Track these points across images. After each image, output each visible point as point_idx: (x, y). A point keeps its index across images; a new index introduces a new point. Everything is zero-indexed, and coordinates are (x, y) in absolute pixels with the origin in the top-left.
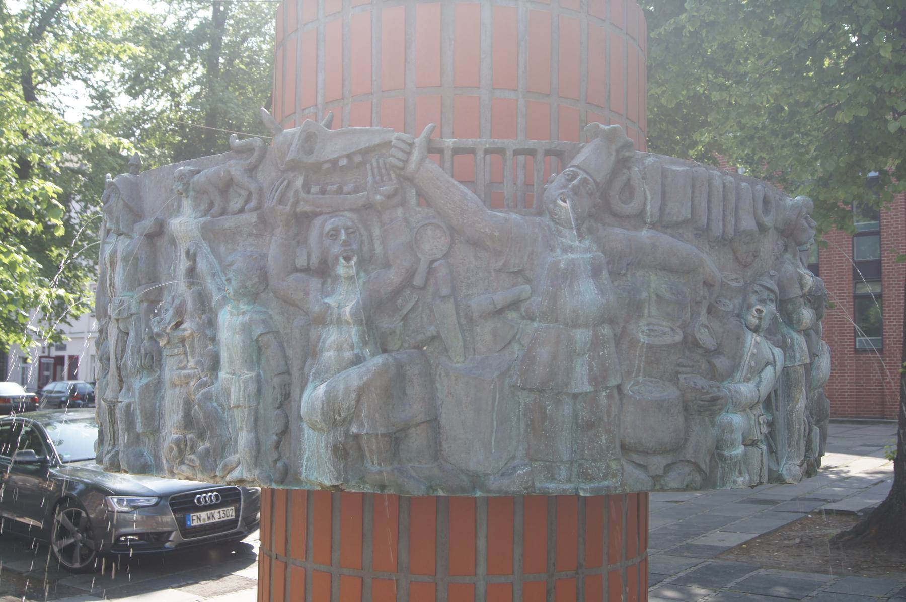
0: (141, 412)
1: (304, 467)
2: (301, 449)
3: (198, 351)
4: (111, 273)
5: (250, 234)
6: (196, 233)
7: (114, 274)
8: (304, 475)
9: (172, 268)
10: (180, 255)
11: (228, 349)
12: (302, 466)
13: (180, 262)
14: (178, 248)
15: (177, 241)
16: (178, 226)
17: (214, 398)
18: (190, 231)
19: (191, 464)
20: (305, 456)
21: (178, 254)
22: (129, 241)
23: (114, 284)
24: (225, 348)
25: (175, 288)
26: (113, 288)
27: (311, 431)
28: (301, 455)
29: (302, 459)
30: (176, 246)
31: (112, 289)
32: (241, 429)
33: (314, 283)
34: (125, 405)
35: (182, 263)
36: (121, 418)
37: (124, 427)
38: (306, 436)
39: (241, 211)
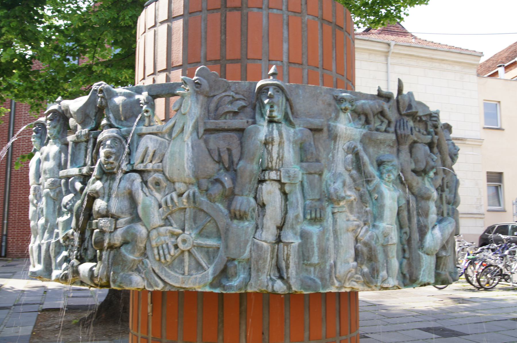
0: (319, 249)
1: (421, 275)
2: (421, 266)
3: (356, 210)
4: (279, 151)
5: (389, 145)
6: (358, 137)
7: (283, 150)
8: (420, 279)
9: (331, 155)
10: (338, 148)
11: (391, 210)
12: (420, 275)
13: (338, 152)
14: (337, 143)
15: (338, 138)
16: (344, 130)
17: (375, 239)
18: (354, 135)
19: (358, 280)
20: (423, 269)
21: (337, 147)
22: (292, 130)
23: (282, 157)
24: (389, 210)
25: (335, 168)
26: (280, 160)
27: (426, 256)
28: (420, 269)
29: (420, 271)
30: (335, 142)
31: (278, 160)
32: (393, 257)
33: (419, 179)
34: (297, 245)
35: (339, 153)
36: (295, 254)
37: (297, 260)
38: (424, 259)
39: (386, 131)
